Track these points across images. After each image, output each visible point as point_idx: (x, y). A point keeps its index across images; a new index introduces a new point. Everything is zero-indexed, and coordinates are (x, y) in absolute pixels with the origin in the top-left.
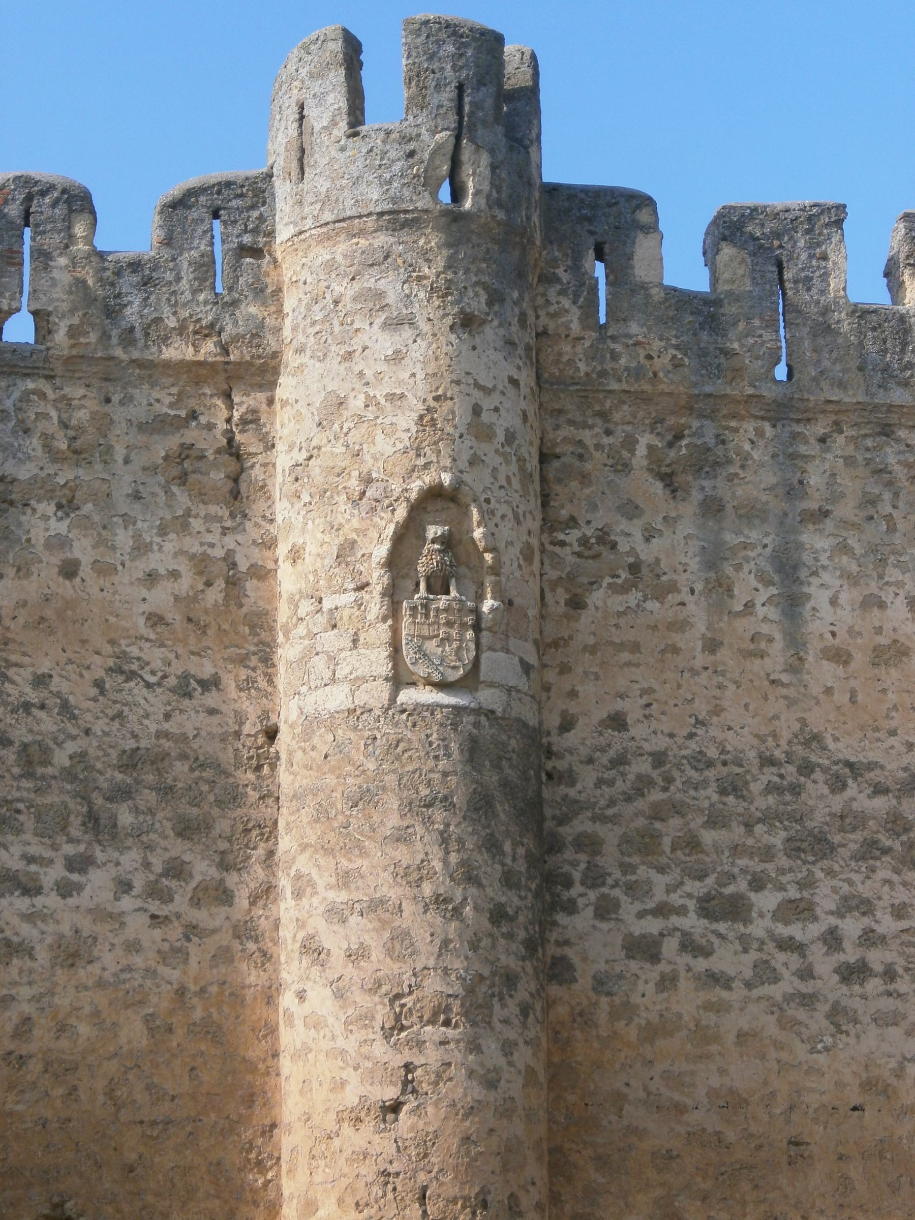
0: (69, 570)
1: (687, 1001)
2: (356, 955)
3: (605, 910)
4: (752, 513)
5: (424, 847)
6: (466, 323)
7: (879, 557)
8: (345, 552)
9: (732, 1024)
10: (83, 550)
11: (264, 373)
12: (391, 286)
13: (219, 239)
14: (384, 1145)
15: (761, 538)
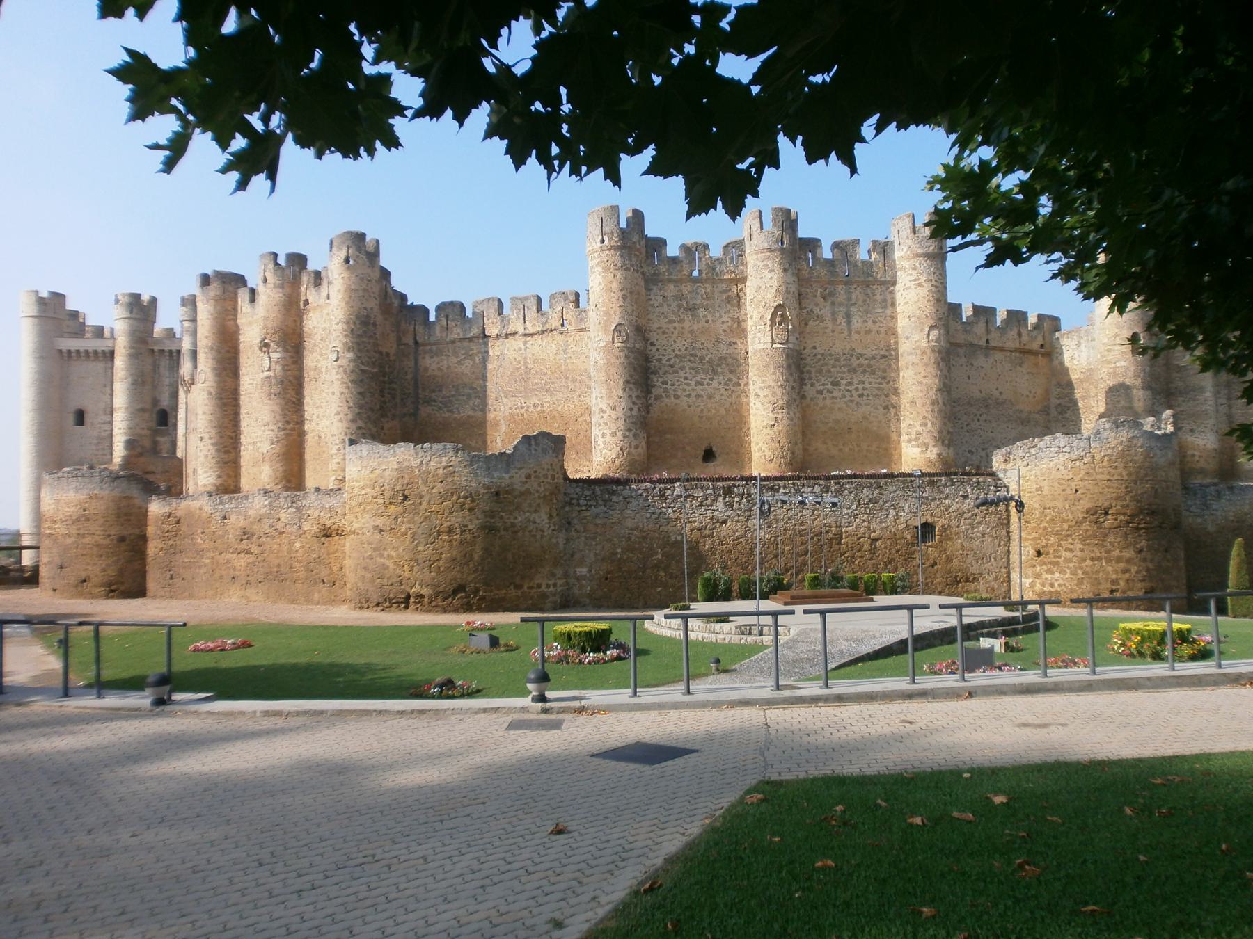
0: (707, 322)
1: (828, 402)
2: (766, 396)
3: (812, 385)
4: (841, 304)
5: (778, 375)
6: (785, 270)
7: (866, 312)
8: (762, 317)
9: (837, 406)
10: (710, 318)
11: (744, 280)
12: (770, 263)
13: (734, 253)
14: (771, 432)
15: (843, 309)
